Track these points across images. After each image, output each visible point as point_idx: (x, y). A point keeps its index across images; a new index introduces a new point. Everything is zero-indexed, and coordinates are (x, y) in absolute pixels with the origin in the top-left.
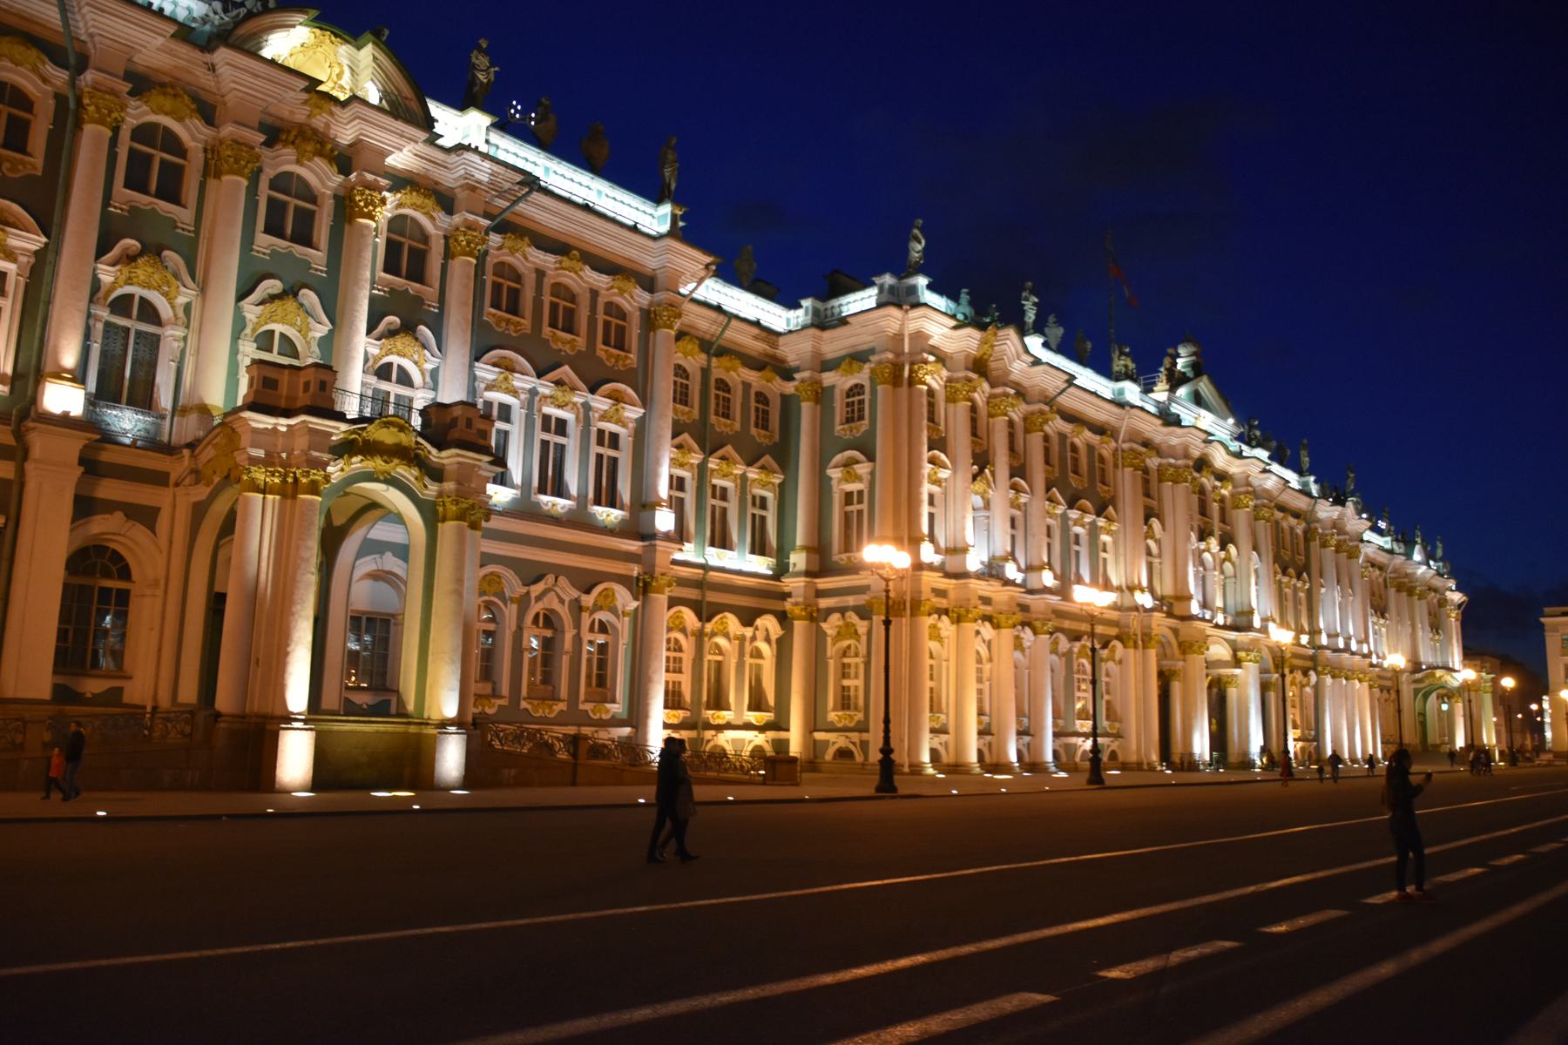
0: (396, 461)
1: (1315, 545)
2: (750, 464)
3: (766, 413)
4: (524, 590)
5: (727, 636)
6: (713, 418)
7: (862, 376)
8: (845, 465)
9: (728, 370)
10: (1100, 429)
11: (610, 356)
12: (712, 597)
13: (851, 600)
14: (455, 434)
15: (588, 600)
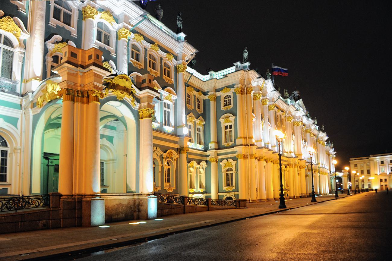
0: (125, 93)
2: (197, 118)
3: (199, 104)
5: (193, 167)
11: (167, 79)
13: (229, 156)
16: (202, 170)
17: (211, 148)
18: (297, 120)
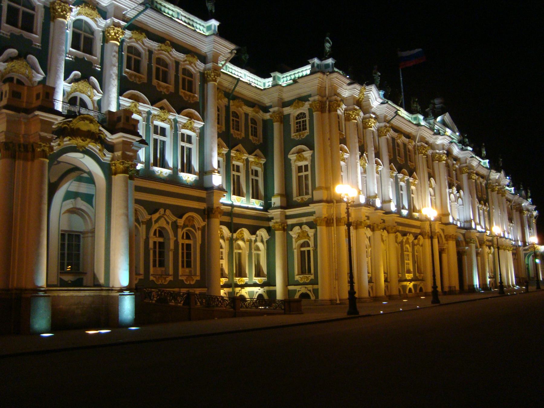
0: (88, 140)
1: (489, 190)
2: (250, 153)
3: (255, 129)
4: (149, 217)
5: (243, 240)
6: (232, 131)
7: (305, 108)
8: (298, 153)
9: (238, 107)
10: (408, 136)
11: (186, 95)
12: (236, 220)
13: (304, 220)
14: (120, 125)
15: (181, 222)
16: (260, 244)
17: (276, 205)
18: (438, 151)
